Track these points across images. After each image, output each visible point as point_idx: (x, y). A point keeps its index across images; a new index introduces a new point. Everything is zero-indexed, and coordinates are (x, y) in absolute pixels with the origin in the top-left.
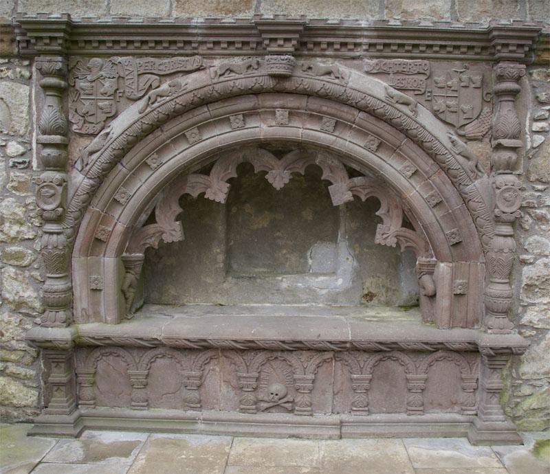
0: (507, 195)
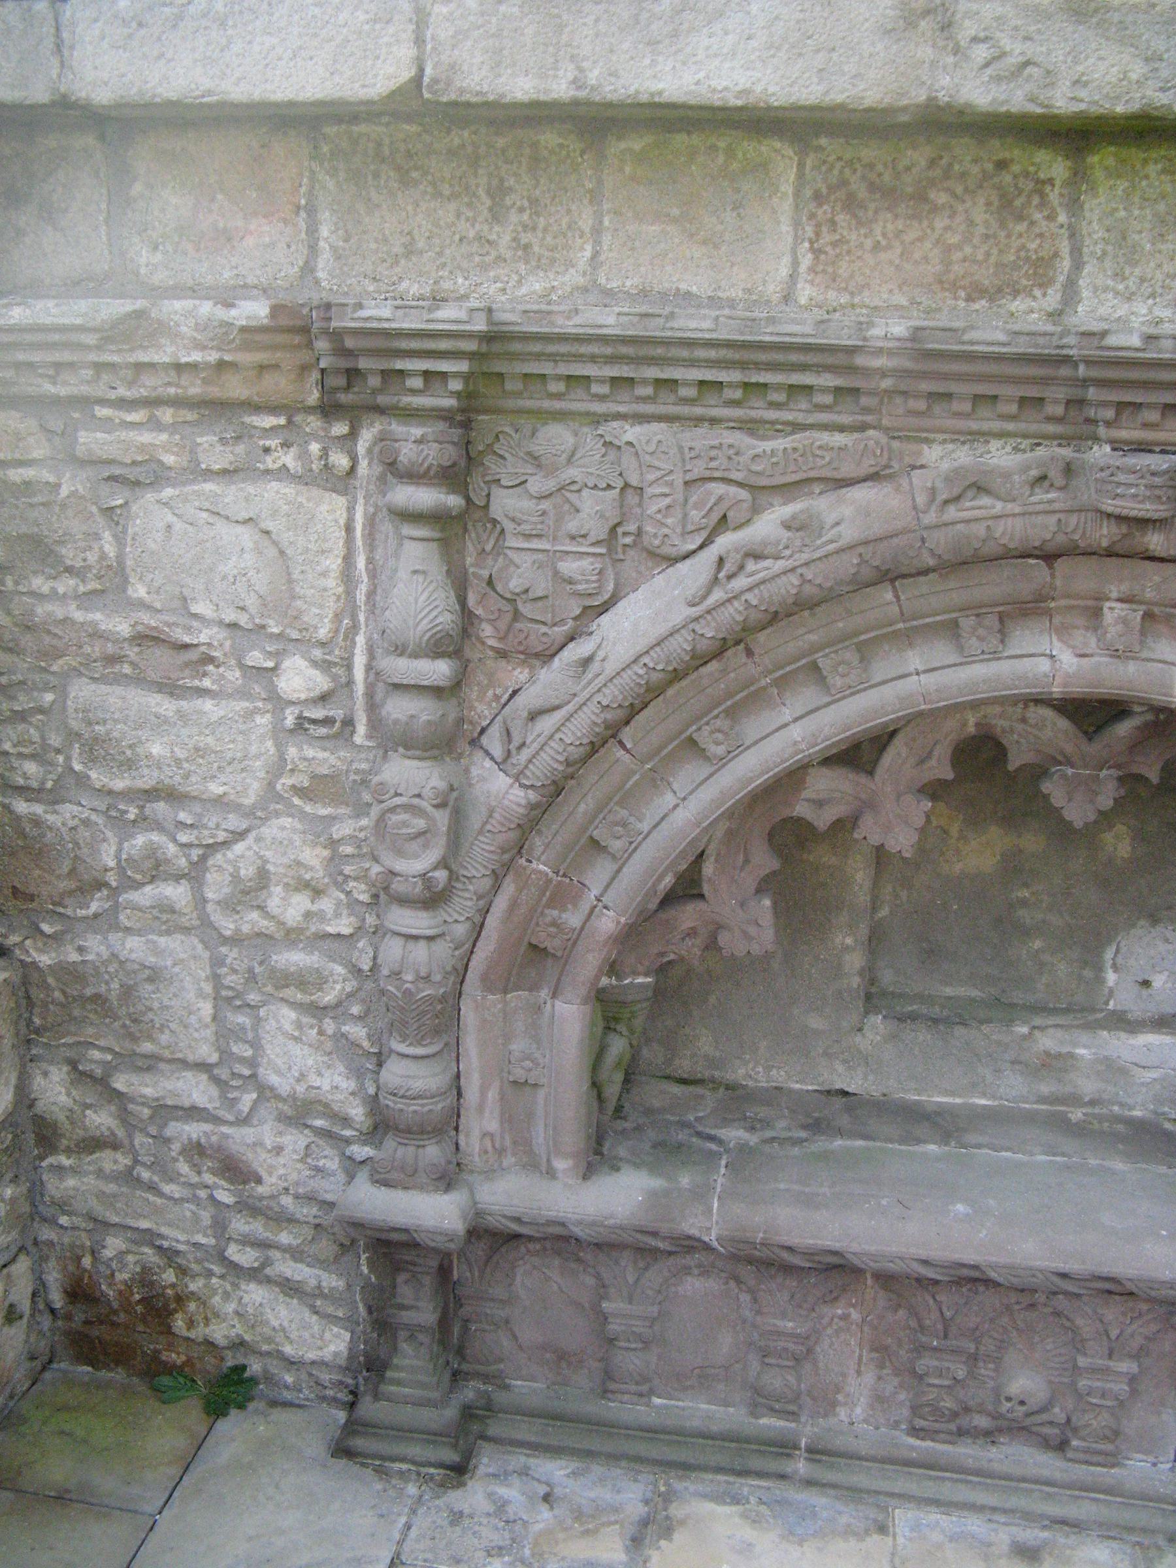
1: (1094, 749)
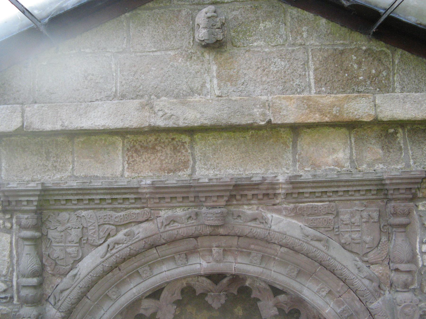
1: (218, 287)
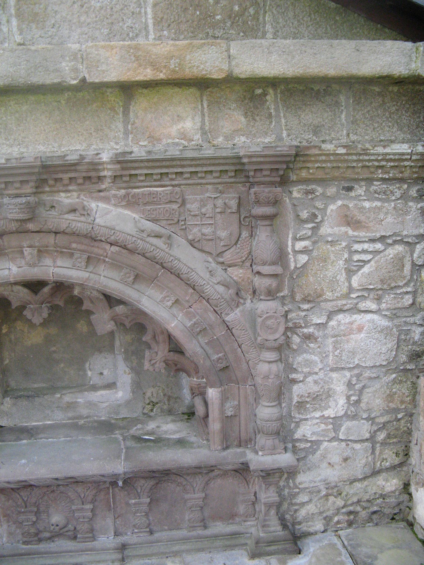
0: (269, 322)
1: (39, 297)
